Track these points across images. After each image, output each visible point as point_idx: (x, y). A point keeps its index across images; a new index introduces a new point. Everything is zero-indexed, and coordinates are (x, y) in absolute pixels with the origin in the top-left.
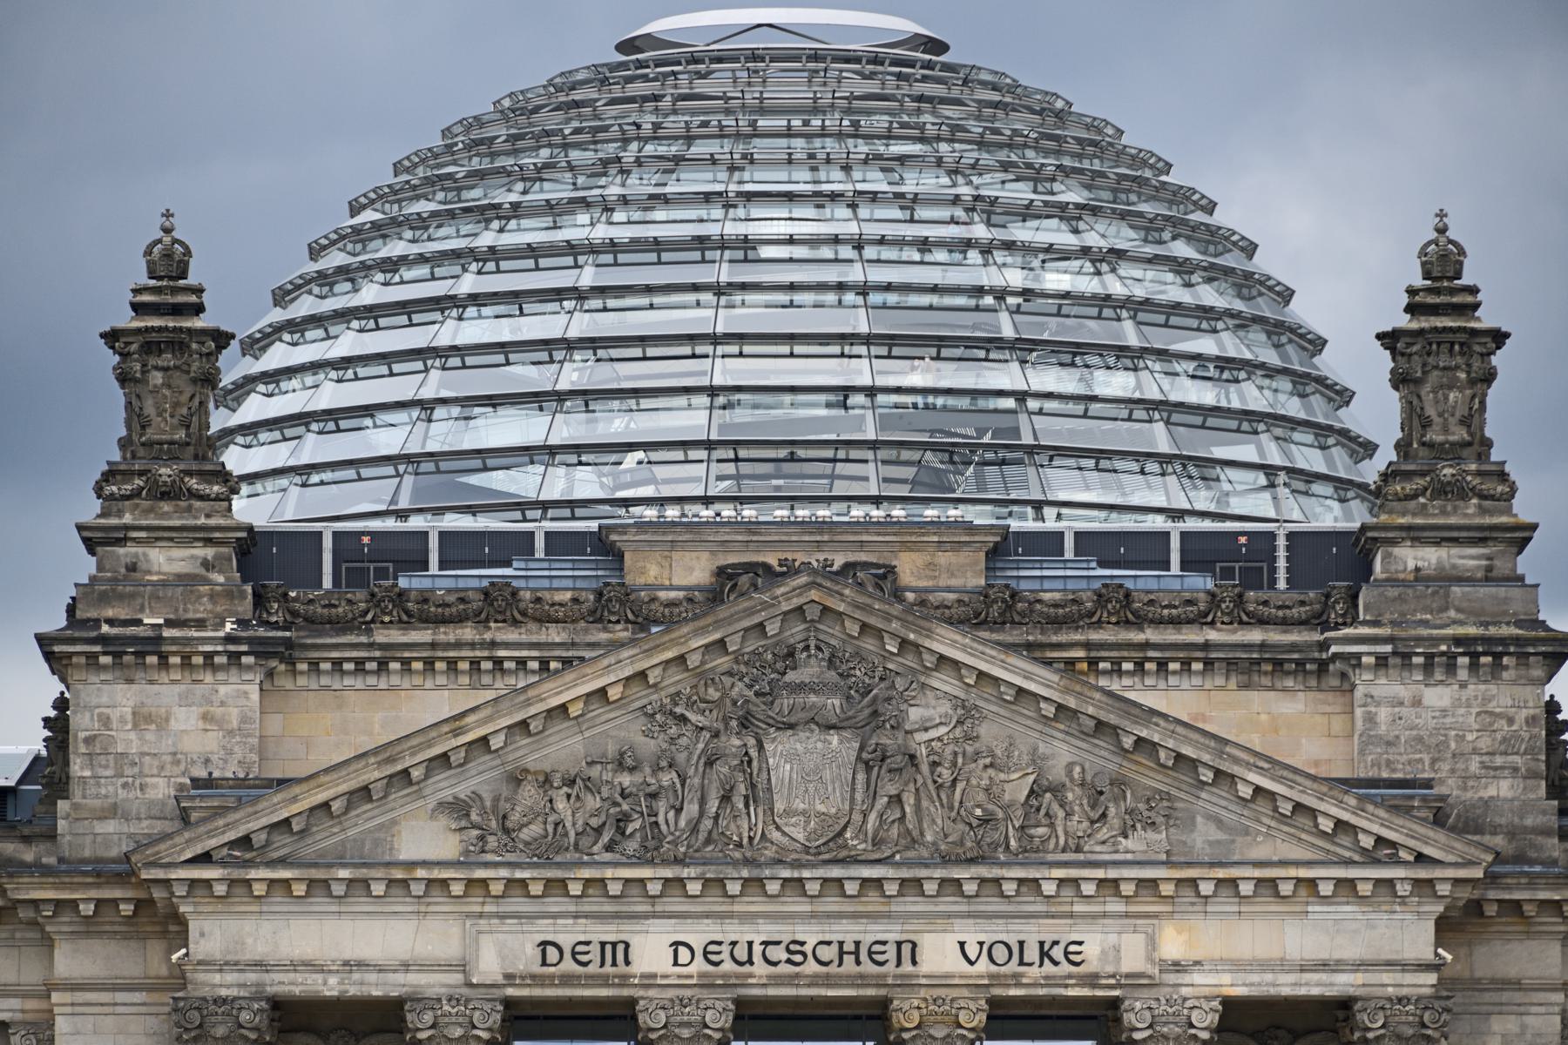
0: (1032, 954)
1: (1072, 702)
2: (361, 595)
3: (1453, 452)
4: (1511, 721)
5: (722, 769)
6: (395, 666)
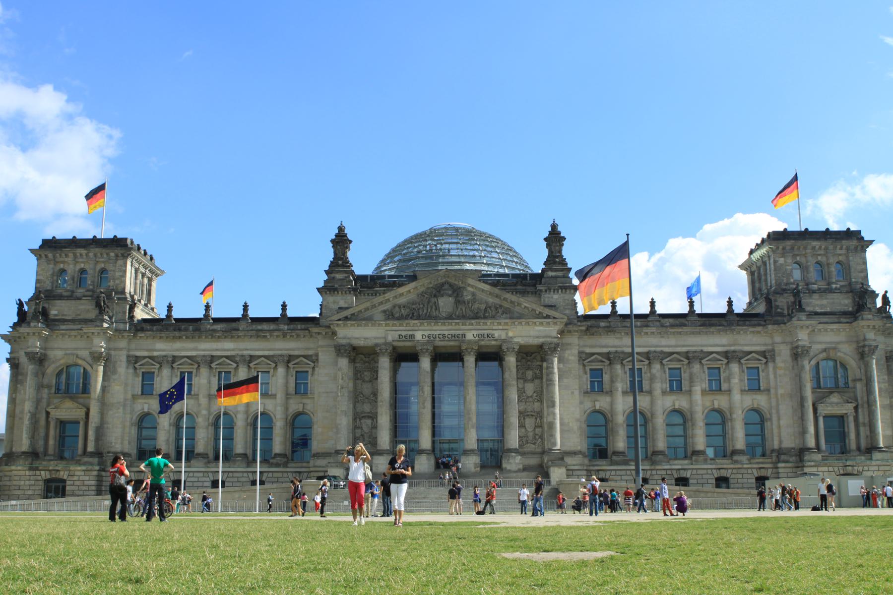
0: (486, 336)
1: (492, 291)
2: (372, 283)
3: (558, 257)
4: (568, 300)
5: (431, 304)
6: (378, 294)
